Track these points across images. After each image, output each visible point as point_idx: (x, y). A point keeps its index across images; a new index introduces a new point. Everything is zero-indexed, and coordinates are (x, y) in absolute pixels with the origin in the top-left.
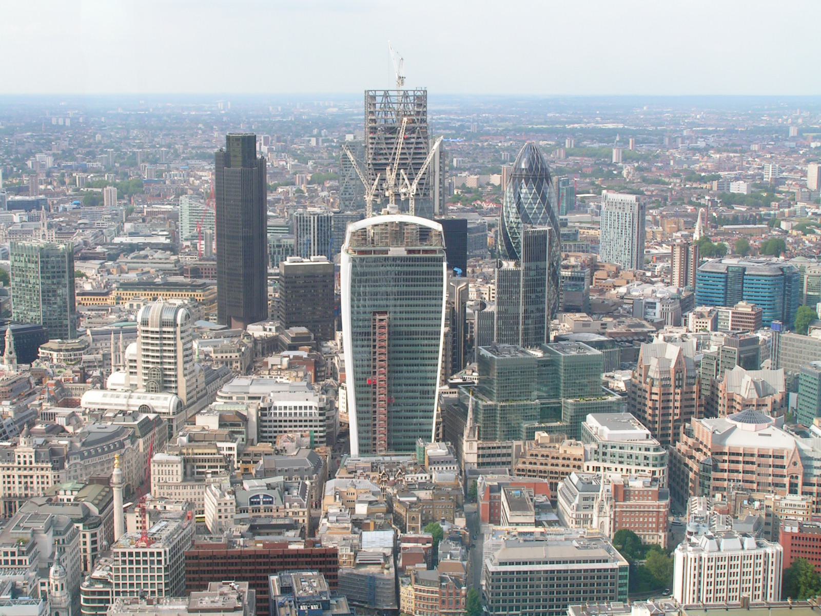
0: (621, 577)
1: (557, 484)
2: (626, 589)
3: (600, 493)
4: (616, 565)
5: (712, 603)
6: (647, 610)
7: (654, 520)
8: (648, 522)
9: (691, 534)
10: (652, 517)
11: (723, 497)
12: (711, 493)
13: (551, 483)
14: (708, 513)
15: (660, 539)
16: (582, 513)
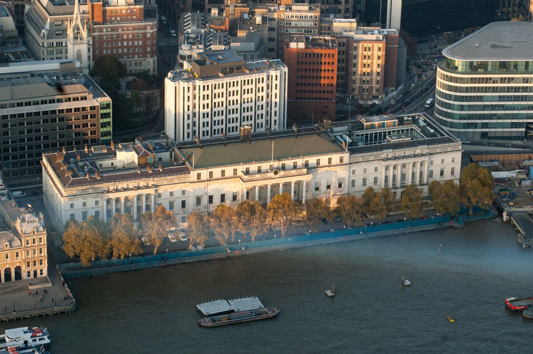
0: (104, 116)
1: (23, 7)
2: (110, 129)
3: (74, 16)
4: (97, 102)
5: (209, 137)
6: (134, 153)
7: (141, 43)
8: (134, 47)
9: (183, 58)
10: (138, 40)
11: (221, 11)
12: (207, 6)
13: (16, 6)
14: (203, 31)
15: (150, 63)
16: (55, 41)
